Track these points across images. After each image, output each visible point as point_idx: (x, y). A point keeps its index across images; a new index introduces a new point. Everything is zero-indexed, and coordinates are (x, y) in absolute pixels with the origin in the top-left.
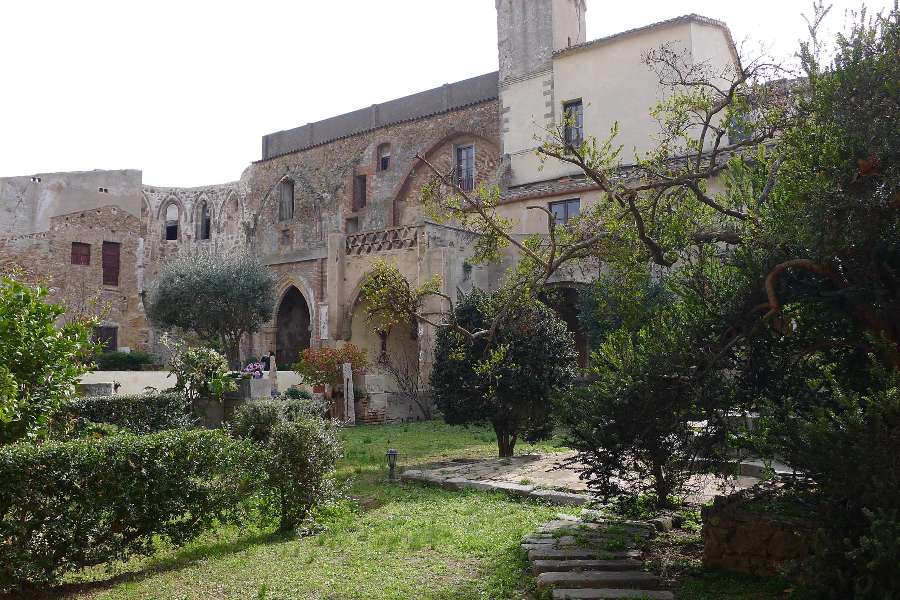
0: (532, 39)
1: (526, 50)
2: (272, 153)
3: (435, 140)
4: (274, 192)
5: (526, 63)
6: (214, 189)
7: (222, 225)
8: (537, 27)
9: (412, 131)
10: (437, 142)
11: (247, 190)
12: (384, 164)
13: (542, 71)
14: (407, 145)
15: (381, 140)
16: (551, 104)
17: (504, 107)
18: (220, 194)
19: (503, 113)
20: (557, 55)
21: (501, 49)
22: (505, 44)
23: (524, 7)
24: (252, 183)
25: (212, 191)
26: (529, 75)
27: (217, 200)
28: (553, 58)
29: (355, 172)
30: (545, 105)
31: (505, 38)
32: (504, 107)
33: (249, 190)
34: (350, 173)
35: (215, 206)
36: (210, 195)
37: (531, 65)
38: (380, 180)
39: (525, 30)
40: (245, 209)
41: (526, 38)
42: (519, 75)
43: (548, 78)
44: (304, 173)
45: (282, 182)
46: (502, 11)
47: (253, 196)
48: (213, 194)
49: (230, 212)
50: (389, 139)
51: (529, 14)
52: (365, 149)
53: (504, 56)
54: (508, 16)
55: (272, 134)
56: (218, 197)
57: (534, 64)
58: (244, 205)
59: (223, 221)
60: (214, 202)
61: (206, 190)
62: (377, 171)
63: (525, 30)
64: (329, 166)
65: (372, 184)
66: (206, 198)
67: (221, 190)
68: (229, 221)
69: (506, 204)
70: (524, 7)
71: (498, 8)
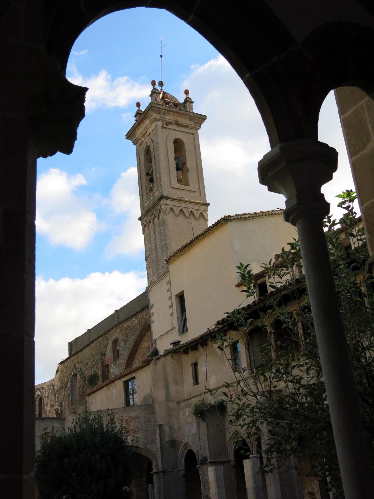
0: (160, 251)
1: (157, 261)
2: (73, 353)
3: (137, 333)
4: (69, 384)
5: (158, 270)
6: (43, 386)
7: (48, 413)
8: (161, 243)
9: (128, 326)
10: (139, 333)
11: (57, 384)
12: (116, 354)
13: (165, 274)
14: (126, 338)
15: (114, 337)
16: (170, 298)
17: (151, 304)
18: (46, 389)
19: (151, 309)
20: (169, 261)
21: (147, 262)
22: (148, 258)
23: (155, 231)
24: (61, 379)
25: (43, 388)
26: (160, 277)
27: (45, 393)
28: (167, 264)
29: (103, 363)
30: (168, 299)
31: (148, 254)
32: (151, 304)
33: (59, 384)
34: (100, 364)
35: (44, 399)
36: (41, 390)
37: (160, 271)
38: (115, 367)
39: (156, 245)
40: (57, 398)
41: (157, 252)
42: (156, 279)
43: (167, 279)
44: (82, 367)
45: (72, 376)
46: (146, 235)
47: (60, 388)
48: (43, 390)
49: (52, 402)
50: (117, 336)
51: (157, 234)
52: (107, 345)
53: (148, 266)
54: (148, 238)
55: (73, 341)
56: (46, 391)
57: (161, 270)
58: (57, 396)
59: (48, 410)
60: (44, 395)
61: (39, 388)
62: (113, 360)
63: (156, 247)
64: (92, 360)
65: (112, 372)
66: (40, 394)
67: (48, 386)
68: (51, 409)
69: (106, 385)
70: (155, 231)
71: (144, 234)
